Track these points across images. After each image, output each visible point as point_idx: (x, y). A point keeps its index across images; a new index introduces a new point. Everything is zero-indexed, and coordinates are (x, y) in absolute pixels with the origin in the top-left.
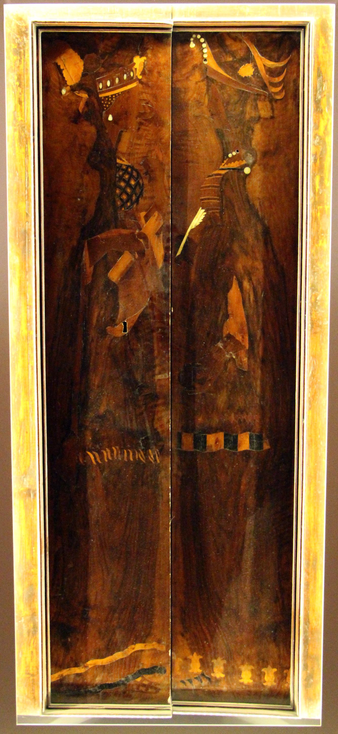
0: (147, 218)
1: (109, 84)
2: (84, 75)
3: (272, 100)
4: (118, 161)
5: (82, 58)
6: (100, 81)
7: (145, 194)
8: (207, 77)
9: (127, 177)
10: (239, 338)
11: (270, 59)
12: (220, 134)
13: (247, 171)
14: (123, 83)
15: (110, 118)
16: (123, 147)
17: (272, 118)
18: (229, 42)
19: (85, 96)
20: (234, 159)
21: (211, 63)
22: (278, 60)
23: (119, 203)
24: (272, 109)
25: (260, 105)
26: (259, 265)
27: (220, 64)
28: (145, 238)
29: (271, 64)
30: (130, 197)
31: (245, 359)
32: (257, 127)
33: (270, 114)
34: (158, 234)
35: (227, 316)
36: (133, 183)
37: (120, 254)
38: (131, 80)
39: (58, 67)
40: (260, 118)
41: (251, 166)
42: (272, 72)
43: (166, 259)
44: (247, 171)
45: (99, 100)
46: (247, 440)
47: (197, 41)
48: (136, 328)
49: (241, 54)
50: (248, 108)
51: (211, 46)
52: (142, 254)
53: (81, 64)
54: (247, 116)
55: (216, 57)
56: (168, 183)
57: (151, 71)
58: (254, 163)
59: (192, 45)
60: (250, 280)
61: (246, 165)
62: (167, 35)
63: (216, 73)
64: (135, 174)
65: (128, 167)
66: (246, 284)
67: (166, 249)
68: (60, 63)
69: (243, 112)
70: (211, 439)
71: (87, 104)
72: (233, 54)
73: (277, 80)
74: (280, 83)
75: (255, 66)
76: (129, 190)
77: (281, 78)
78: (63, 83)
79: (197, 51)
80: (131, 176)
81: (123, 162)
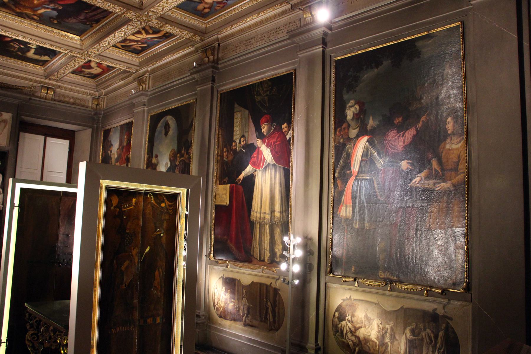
0: (134, 249)
1: (125, 206)
2: (118, 203)
3: (169, 214)
4: (126, 231)
5: (118, 197)
6: (123, 205)
7: (133, 242)
8: (152, 206)
9: (128, 236)
10: (158, 287)
11: (170, 202)
12: (155, 223)
13: (162, 235)
14: (129, 206)
15: (125, 217)
16: (128, 227)
17: (169, 219)
18: (159, 196)
19: (118, 210)
20: (158, 231)
21: (153, 202)
22: (171, 203)
23: (126, 244)
24: (169, 217)
25: (166, 215)
26: (164, 264)
27: (156, 202)
28: (132, 255)
29: (170, 203)
30: (129, 243)
31: (159, 293)
32: (165, 222)
33: (168, 218)
34: (136, 254)
35: (154, 280)
36: (130, 238)
37: (125, 261)
38: (131, 206)
39: (111, 200)
40: (166, 219)
41: (163, 234)
42: (170, 206)
43: (138, 262)
44: (162, 235)
45: (122, 211)
46: (159, 319)
47: (150, 196)
48: (129, 286)
49: (162, 200)
50: (163, 216)
51: (154, 197)
52: (131, 261)
53: (118, 199)
54: (163, 219)
55: (155, 200)
56: (140, 238)
57: (137, 203)
58: (164, 232)
59: (149, 196)
60: (161, 268)
61: (162, 233)
62: (142, 192)
63: (155, 205)
64: (131, 235)
65: (129, 233)
66: (160, 270)
67: (139, 259)
68: (112, 199)
69: (162, 217)
70: (149, 320)
71: (119, 212)
72: (159, 200)
73: (171, 208)
74: (171, 209)
75: (165, 204)
76: (129, 241)
77: (172, 207)
78: (112, 205)
79: (150, 198)
80: (130, 236)
81: (128, 231)
